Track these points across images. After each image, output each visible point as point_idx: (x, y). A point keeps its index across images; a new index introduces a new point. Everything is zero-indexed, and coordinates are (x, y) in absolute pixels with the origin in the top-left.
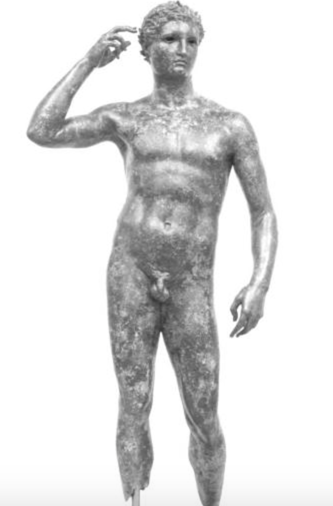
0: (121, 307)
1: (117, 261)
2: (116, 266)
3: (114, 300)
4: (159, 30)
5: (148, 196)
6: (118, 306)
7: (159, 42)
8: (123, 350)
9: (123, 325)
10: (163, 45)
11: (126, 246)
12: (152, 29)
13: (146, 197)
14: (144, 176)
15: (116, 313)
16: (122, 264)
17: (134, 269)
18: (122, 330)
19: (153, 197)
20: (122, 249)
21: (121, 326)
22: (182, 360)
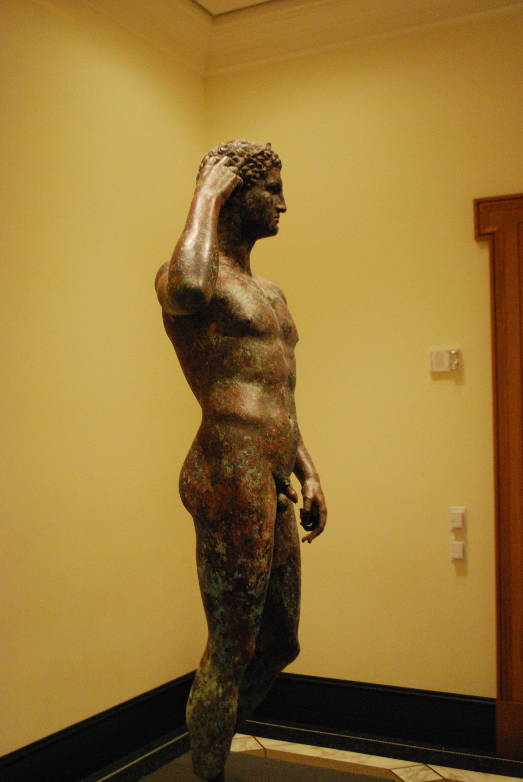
0: (264, 527)
1: (252, 468)
2: (251, 475)
3: (255, 519)
4: (263, 176)
5: (270, 383)
6: (261, 526)
7: (264, 191)
8: (260, 582)
9: (265, 551)
10: (267, 194)
11: (258, 448)
12: (256, 172)
13: (267, 384)
14: (262, 358)
15: (256, 536)
16: (258, 472)
17: (270, 477)
18: (263, 556)
19: (275, 384)
20: (253, 451)
21: (263, 551)
22: (286, 580)
